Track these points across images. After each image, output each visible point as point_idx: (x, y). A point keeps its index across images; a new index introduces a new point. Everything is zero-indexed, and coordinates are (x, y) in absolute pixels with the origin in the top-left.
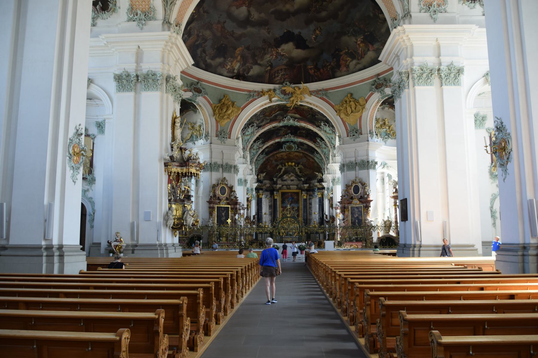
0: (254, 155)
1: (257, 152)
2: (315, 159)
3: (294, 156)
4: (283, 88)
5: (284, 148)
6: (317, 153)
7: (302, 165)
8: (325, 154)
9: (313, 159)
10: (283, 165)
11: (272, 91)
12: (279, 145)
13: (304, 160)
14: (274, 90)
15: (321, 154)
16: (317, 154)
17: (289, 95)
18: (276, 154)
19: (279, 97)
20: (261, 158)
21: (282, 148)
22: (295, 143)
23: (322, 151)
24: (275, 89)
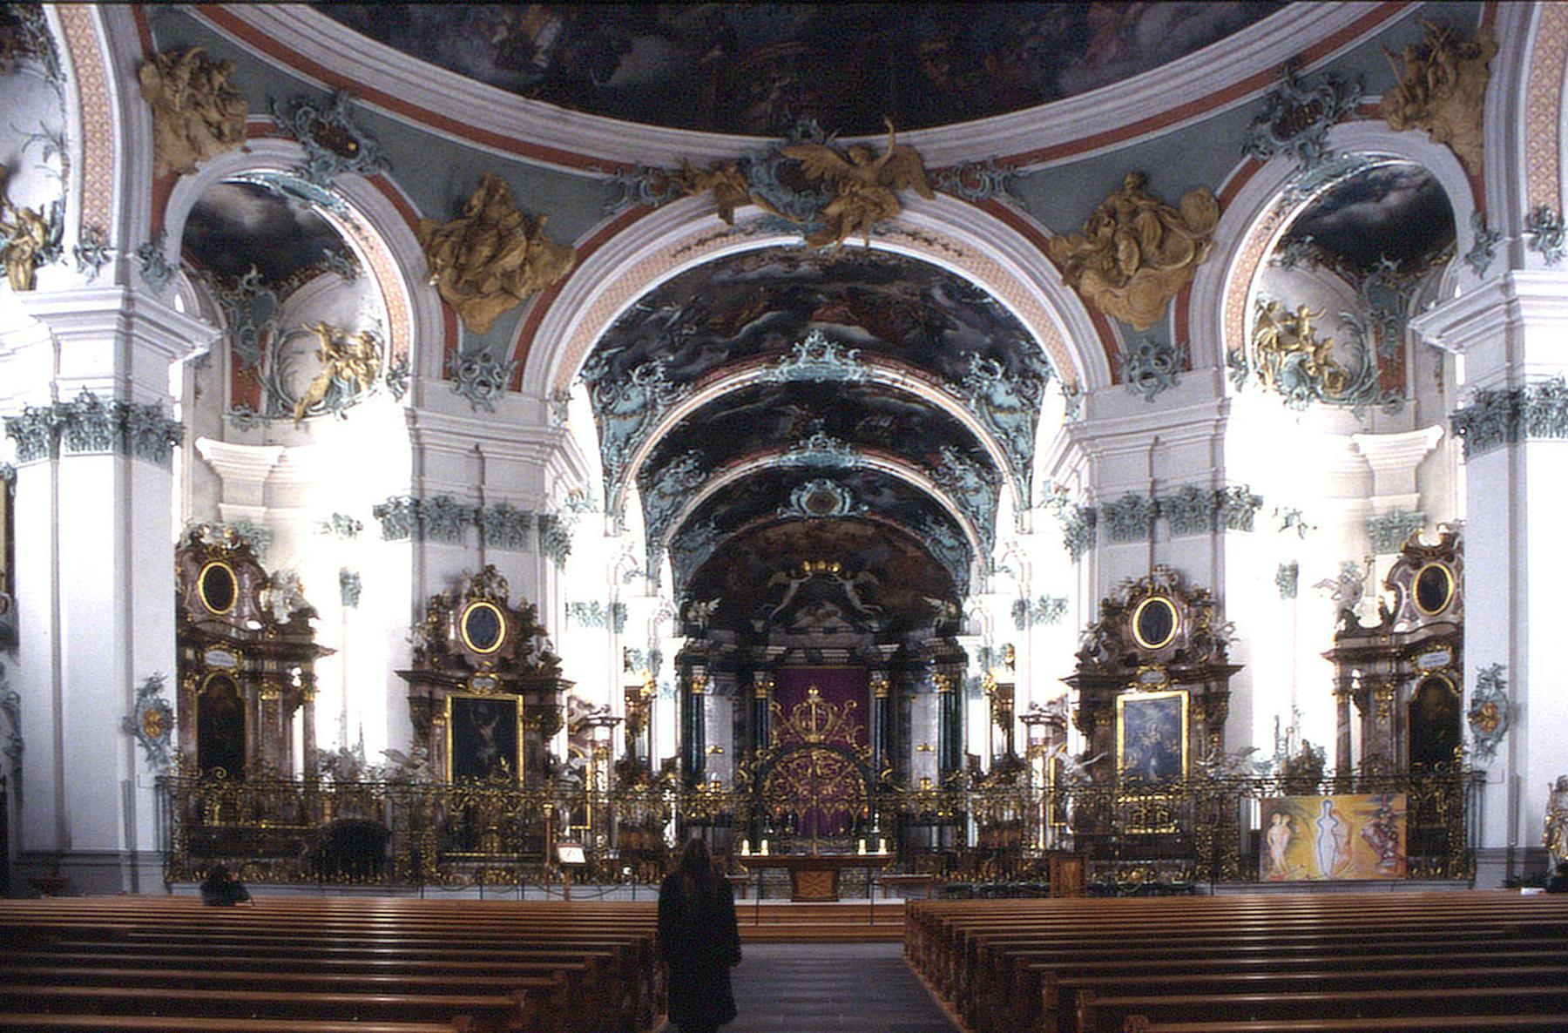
0: (665, 519)
1: (677, 507)
2: (928, 543)
3: (838, 538)
4: (792, 154)
5: (794, 498)
6: (936, 522)
7: (871, 571)
8: (976, 515)
9: (919, 546)
10: (793, 572)
11: (732, 170)
12: (776, 485)
13: (883, 553)
14: (743, 164)
15: (959, 517)
16: (934, 526)
17: (818, 191)
18: (765, 527)
19: (767, 203)
20: (700, 540)
21: (788, 504)
22: (840, 475)
23: (963, 505)
24: (749, 161)
